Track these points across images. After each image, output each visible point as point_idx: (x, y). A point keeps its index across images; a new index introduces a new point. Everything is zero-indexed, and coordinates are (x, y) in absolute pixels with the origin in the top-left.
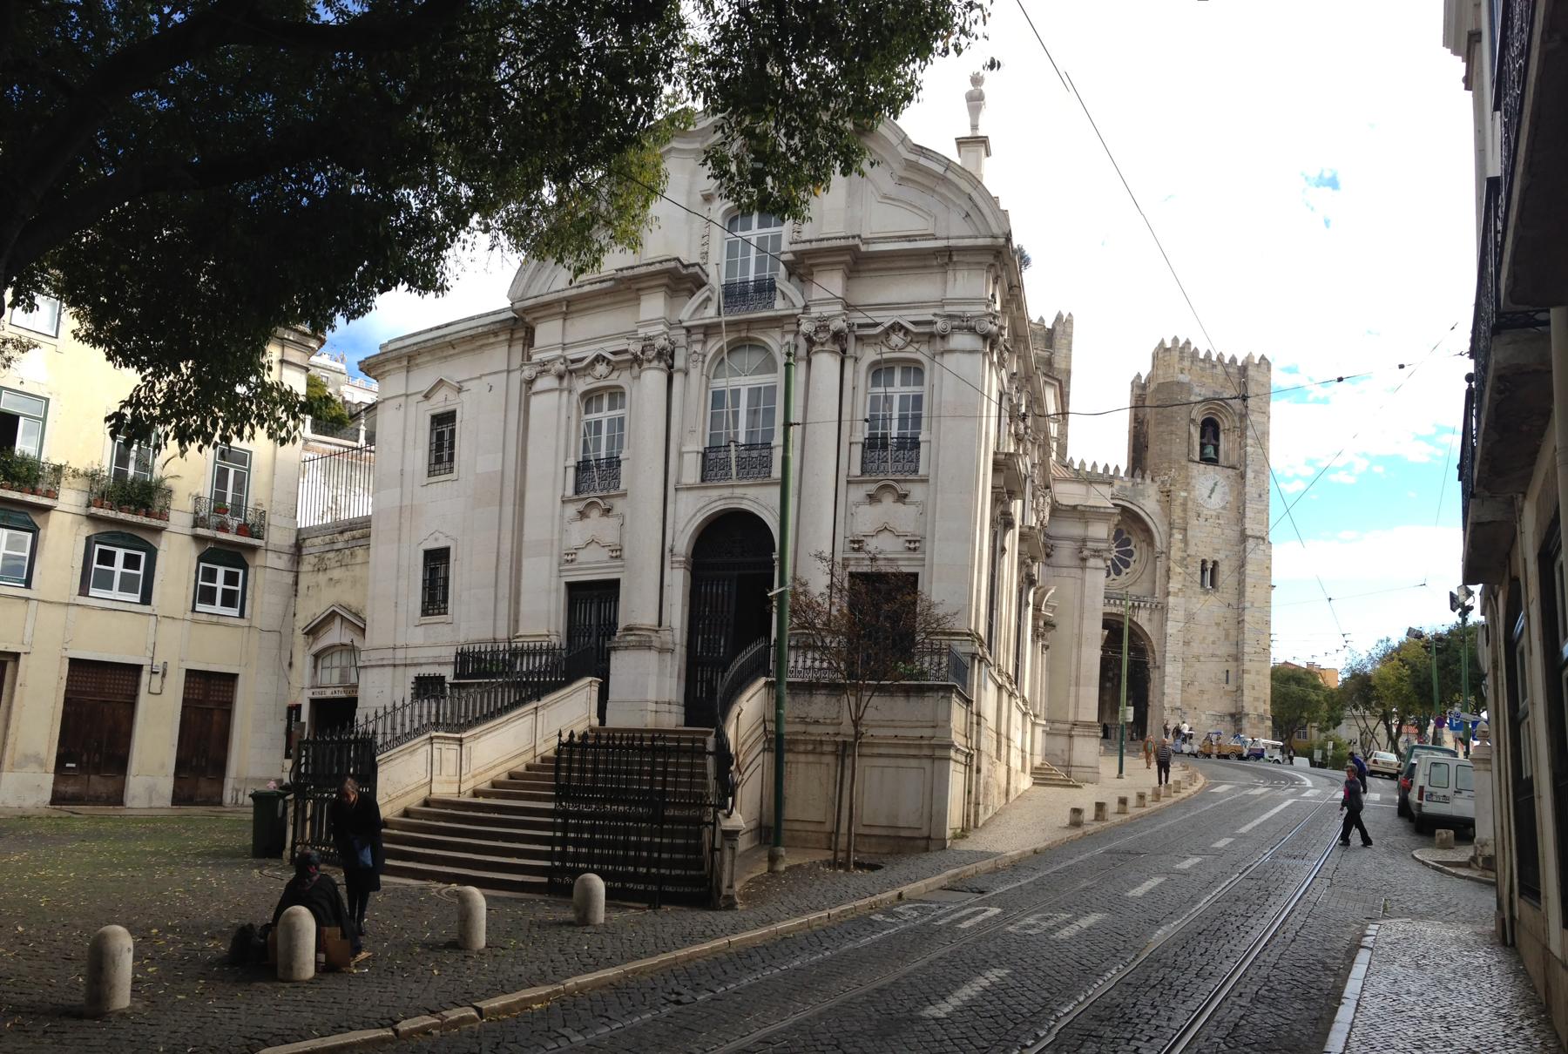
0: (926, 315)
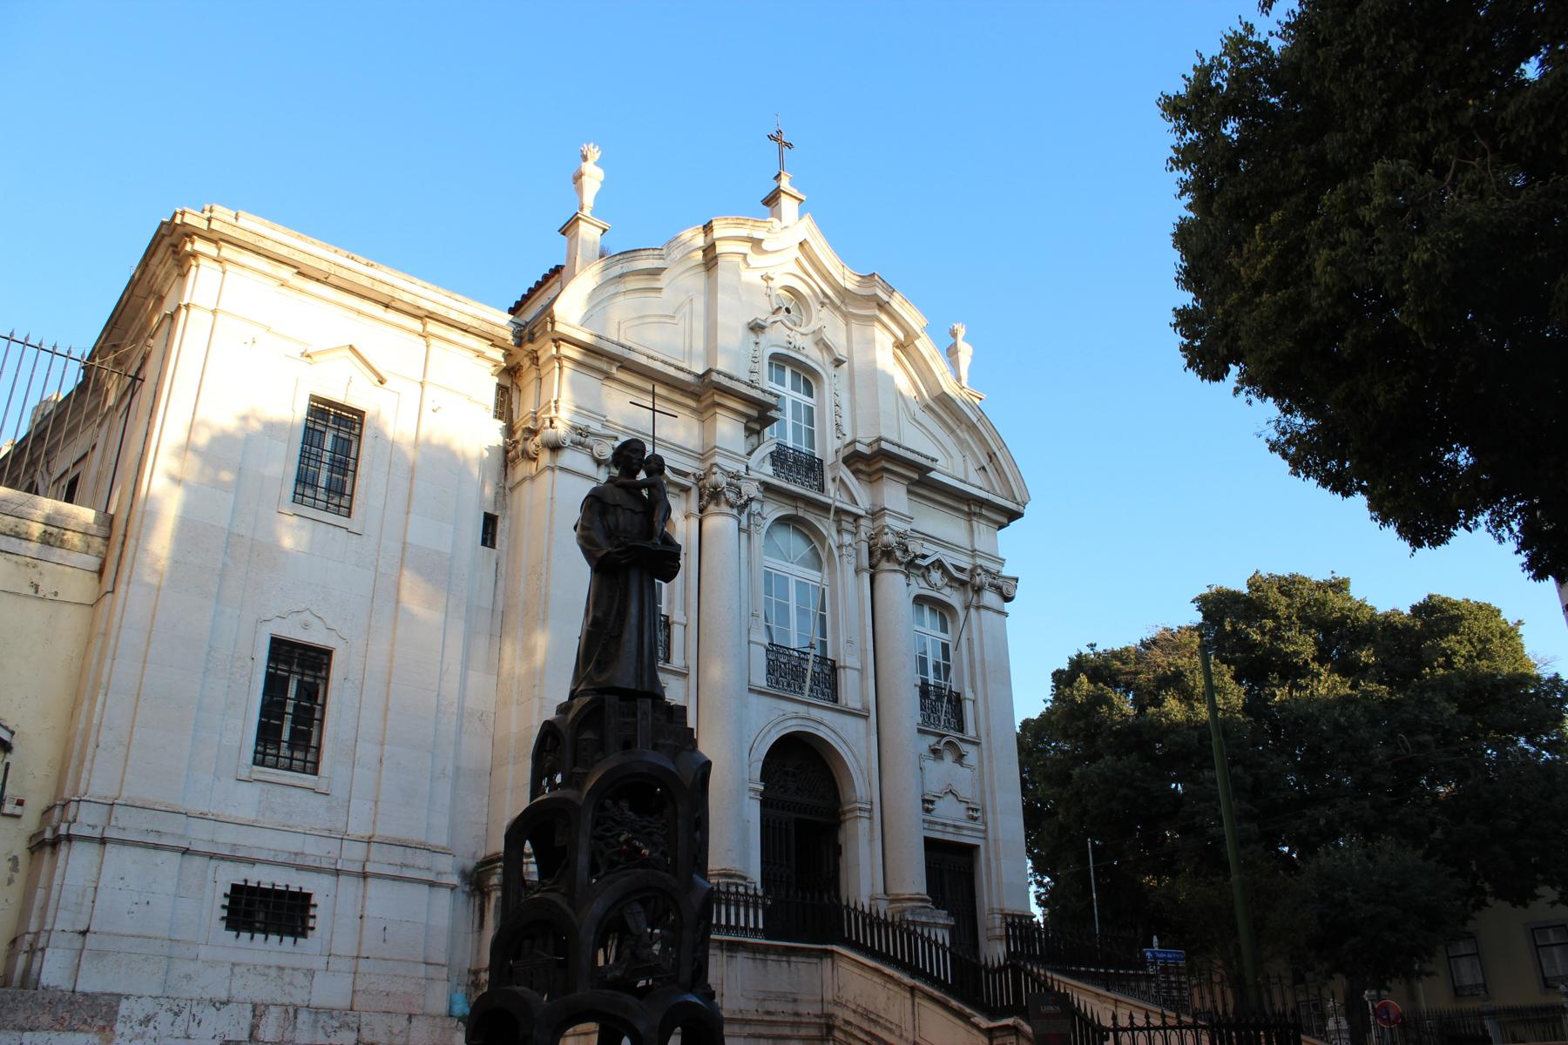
0: (965, 562)
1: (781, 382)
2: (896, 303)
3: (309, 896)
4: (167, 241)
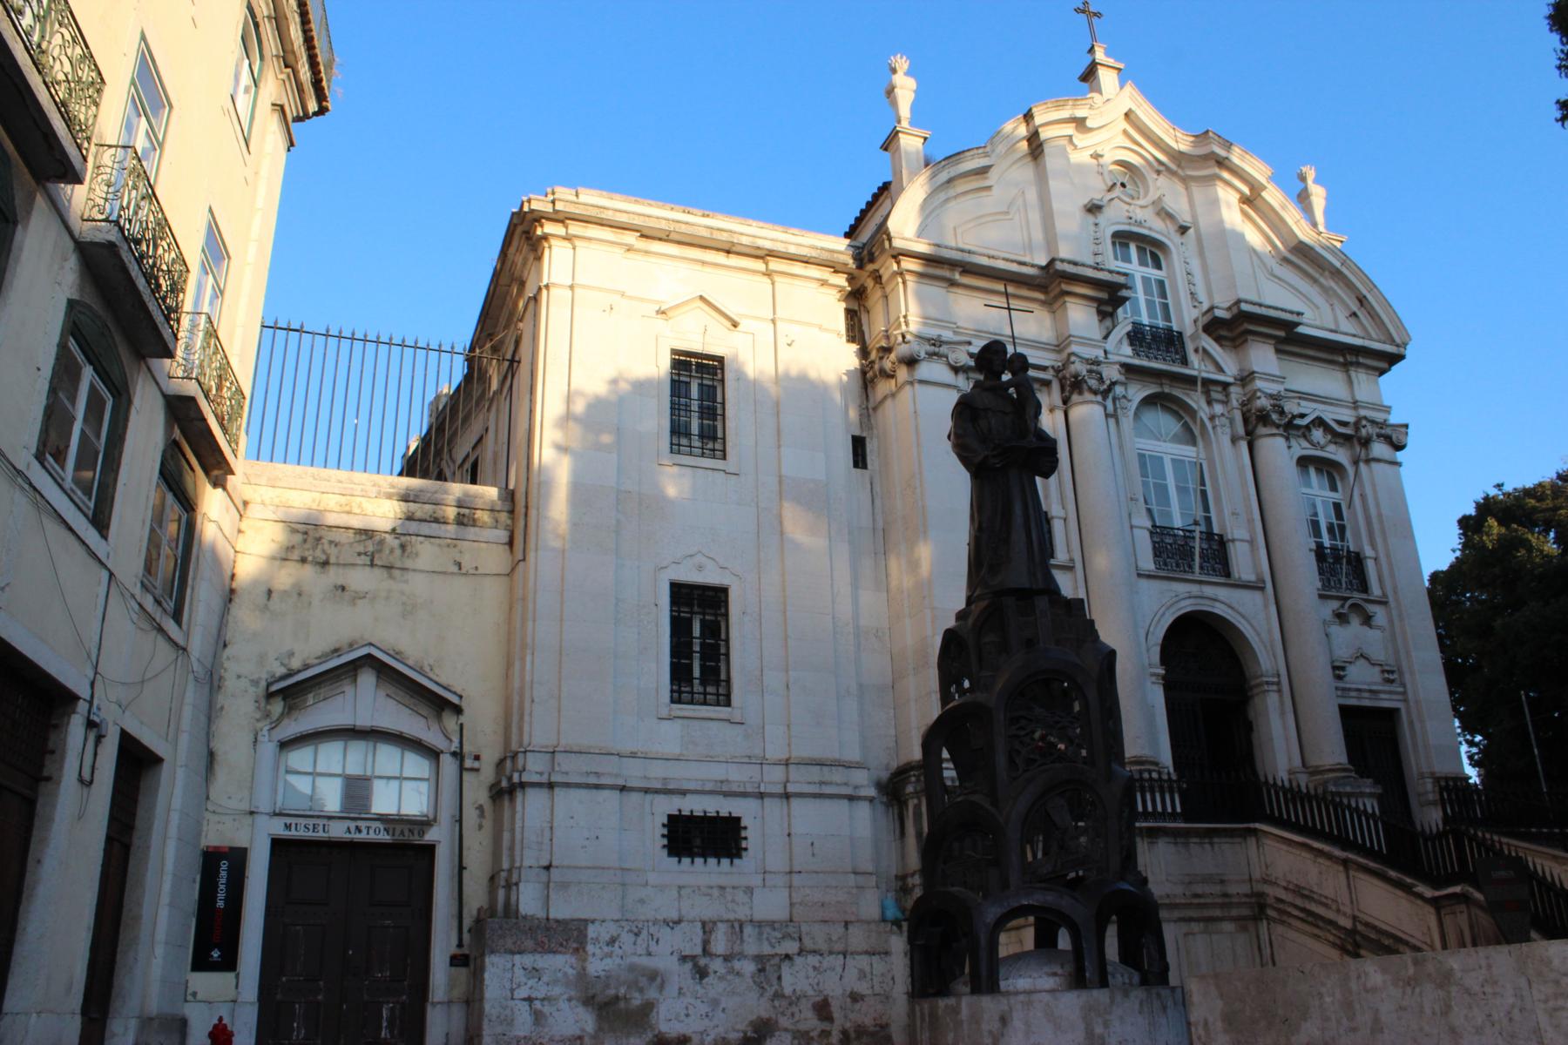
0: (1347, 415)
1: (1127, 260)
2: (1236, 157)
3: (738, 819)
4: (519, 230)
